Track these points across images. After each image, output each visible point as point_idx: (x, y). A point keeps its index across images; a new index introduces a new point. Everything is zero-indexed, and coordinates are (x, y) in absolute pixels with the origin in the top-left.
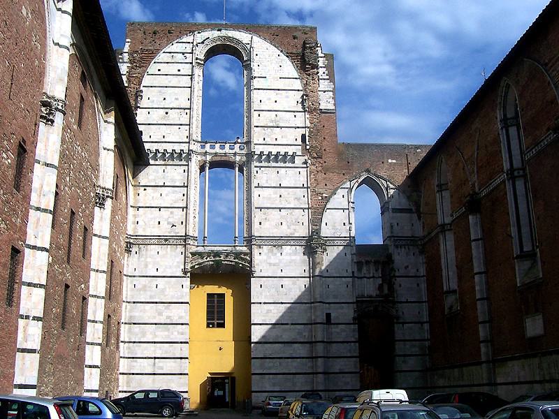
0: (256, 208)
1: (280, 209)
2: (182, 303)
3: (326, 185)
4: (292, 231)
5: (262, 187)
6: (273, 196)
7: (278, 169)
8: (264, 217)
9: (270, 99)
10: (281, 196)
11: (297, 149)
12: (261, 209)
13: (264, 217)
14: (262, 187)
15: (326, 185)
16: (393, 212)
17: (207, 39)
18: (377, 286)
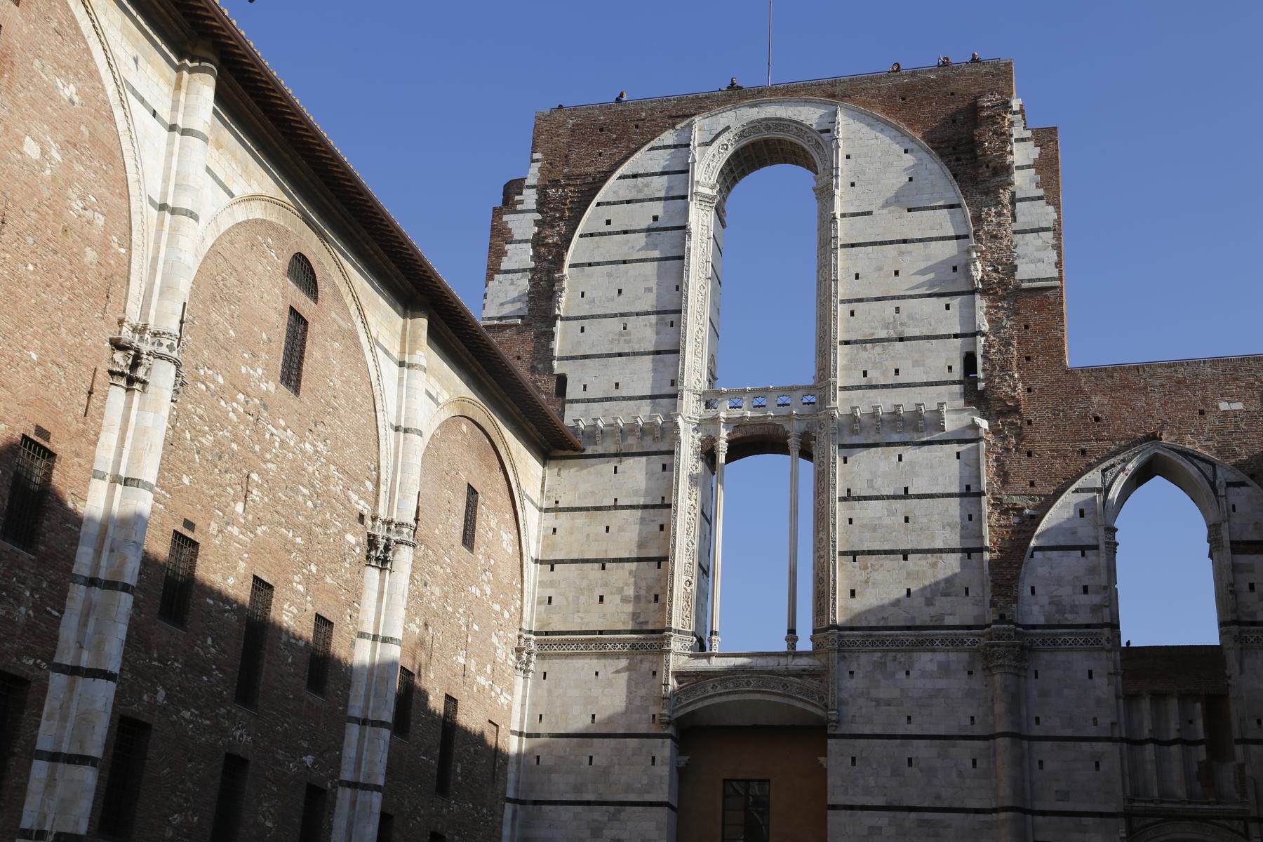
0: (843, 553)
1: (905, 554)
2: (651, 804)
3: (1032, 484)
4: (933, 611)
5: (860, 498)
6: (887, 521)
7: (900, 449)
8: (861, 576)
9: (880, 269)
10: (907, 520)
11: (950, 394)
12: (854, 554)
13: (861, 576)
14: (860, 498)
15: (1032, 484)
16: (1233, 552)
17: (724, 131)
18: (1195, 768)
